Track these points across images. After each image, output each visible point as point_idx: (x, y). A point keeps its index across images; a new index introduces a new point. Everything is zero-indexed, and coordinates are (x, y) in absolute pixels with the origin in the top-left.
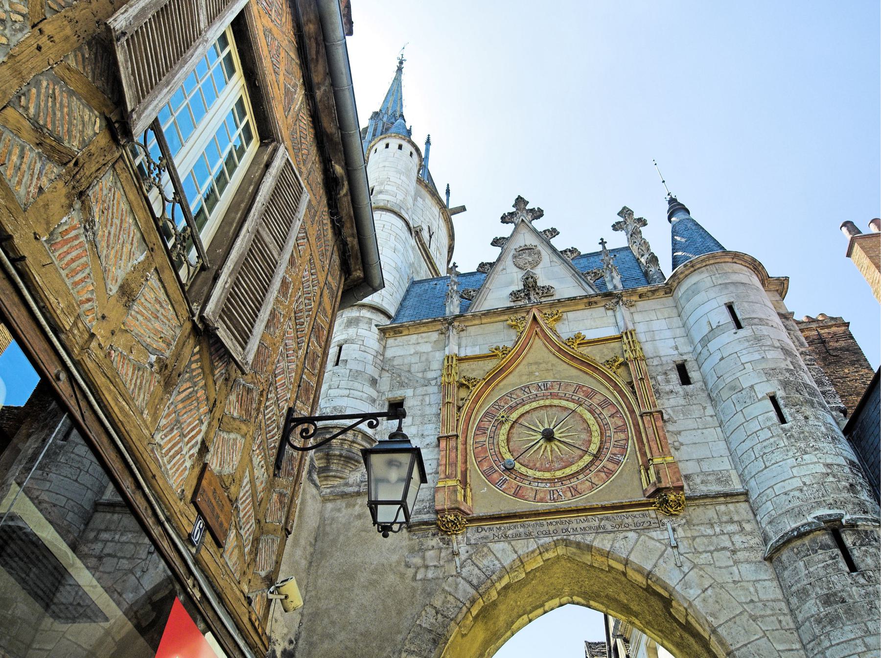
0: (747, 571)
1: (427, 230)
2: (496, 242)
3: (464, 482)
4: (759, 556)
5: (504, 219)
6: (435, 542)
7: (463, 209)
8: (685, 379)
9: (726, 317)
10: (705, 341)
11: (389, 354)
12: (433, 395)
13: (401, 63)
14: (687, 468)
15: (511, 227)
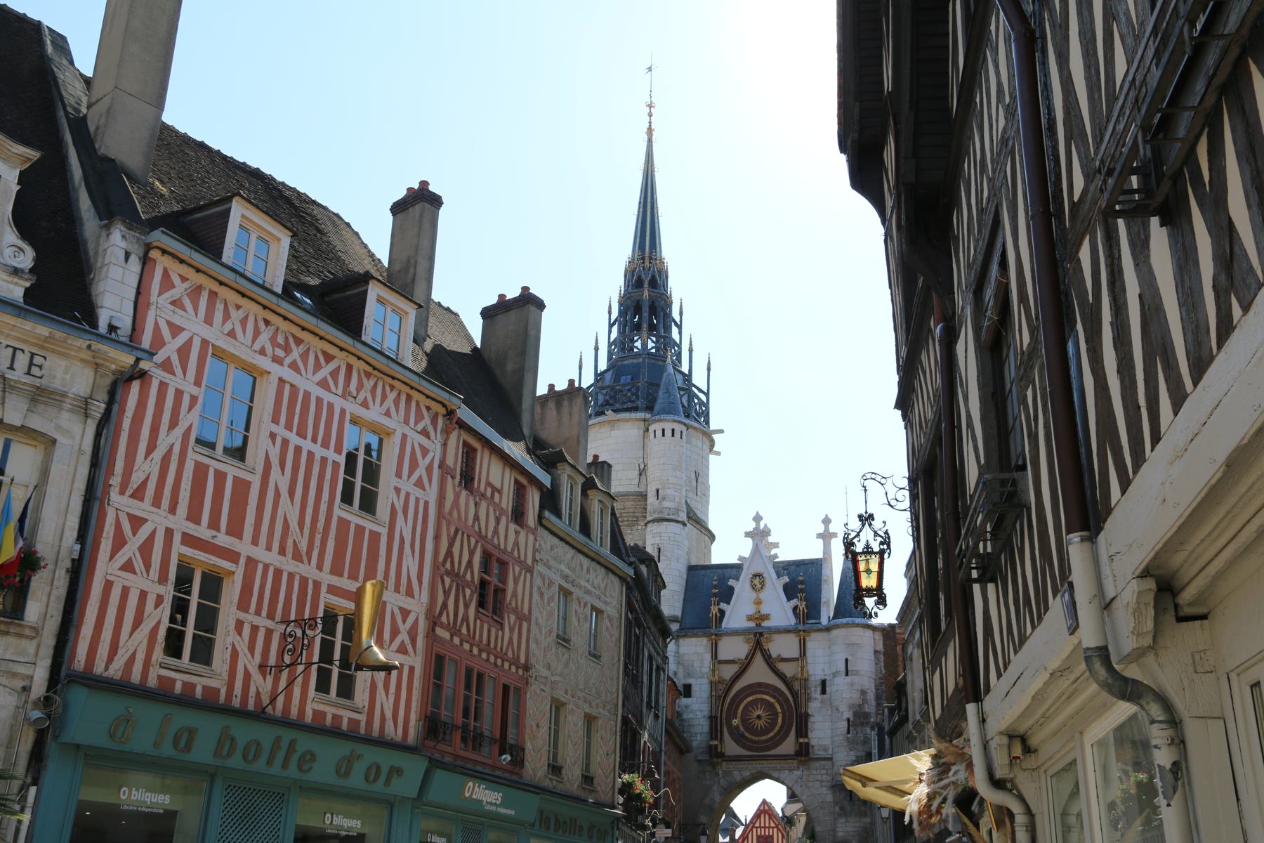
0: (824, 790)
1: (693, 476)
2: (741, 558)
3: (721, 740)
4: (828, 784)
5: (748, 534)
6: (708, 768)
7: (721, 431)
8: (824, 692)
9: (843, 669)
10: (835, 675)
11: (682, 650)
12: (706, 687)
13: (650, 115)
14: (813, 742)
15: (749, 541)
